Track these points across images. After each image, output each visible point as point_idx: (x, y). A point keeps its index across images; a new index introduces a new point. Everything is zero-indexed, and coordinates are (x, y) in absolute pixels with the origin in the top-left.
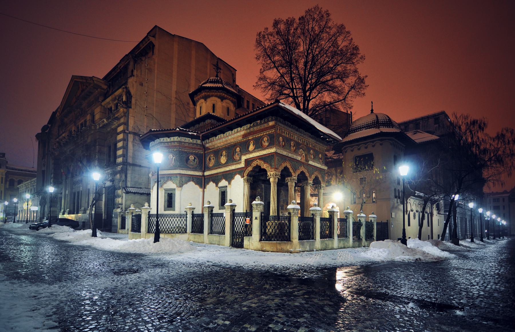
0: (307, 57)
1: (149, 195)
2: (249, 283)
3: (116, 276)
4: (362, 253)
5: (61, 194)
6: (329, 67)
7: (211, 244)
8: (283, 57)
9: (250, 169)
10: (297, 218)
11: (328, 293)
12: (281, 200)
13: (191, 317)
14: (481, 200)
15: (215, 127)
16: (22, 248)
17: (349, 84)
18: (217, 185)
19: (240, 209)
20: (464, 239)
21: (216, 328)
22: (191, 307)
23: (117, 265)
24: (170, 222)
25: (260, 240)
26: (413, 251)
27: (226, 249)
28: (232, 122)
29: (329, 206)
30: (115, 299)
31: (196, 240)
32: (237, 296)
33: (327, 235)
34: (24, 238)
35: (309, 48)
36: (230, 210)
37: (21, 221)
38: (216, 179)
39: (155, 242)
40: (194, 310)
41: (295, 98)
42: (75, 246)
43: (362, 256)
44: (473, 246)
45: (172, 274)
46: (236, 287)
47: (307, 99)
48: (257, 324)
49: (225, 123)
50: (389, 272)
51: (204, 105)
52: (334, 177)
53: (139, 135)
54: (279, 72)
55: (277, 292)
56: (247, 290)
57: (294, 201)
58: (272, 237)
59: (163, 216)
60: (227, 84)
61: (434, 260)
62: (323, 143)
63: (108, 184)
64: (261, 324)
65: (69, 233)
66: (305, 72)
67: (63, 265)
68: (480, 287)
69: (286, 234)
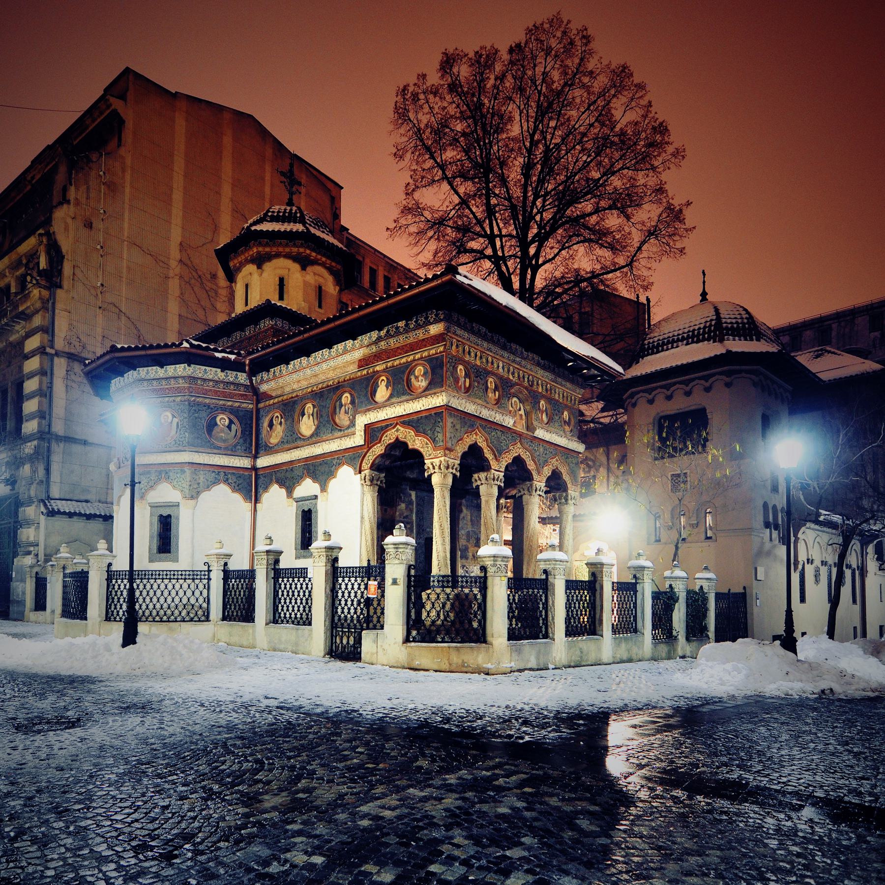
2: (377, 754)
10: (506, 580)
11: (587, 780)
12: (462, 533)
13: (222, 844)
15: (284, 340)
18: (290, 493)
19: (354, 555)
21: (286, 873)
24: (166, 593)
25: (407, 640)
28: (332, 325)
31: (235, 639)
32: (344, 789)
36: (324, 559)
39: (124, 645)
40: (230, 827)
45: (171, 730)
48: (397, 863)
49: (311, 329)
52: (603, 471)
55: (452, 779)
56: (371, 772)
57: (496, 536)
59: (146, 575)
62: (572, 382)
64: (408, 863)
69: (475, 625)
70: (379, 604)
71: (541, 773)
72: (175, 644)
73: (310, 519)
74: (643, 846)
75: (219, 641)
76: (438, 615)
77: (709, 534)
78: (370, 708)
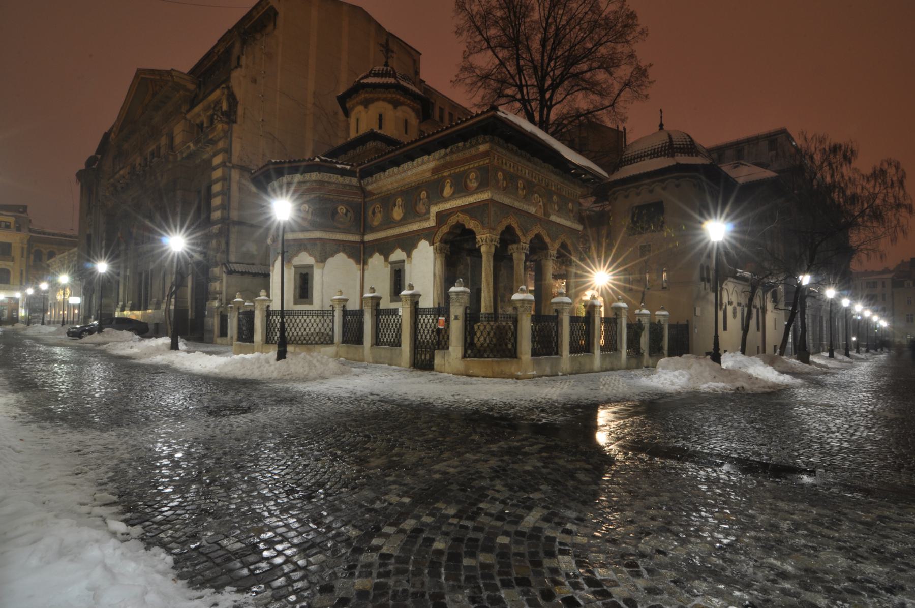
0: (545, 29)
1: (267, 276)
3: (212, 419)
5: (119, 274)
7: (377, 363)
8: (504, 30)
9: (445, 229)
10: (529, 317)
12: (501, 285)
14: (846, 282)
15: (382, 155)
16: (56, 367)
17: (621, 78)
18: (386, 259)
19: (428, 301)
20: (818, 352)
22: (343, 473)
23: (213, 399)
24: (305, 325)
30: (210, 458)
33: (582, 347)
34: (59, 352)
37: (54, 322)
41: (525, 102)
42: (143, 365)
43: (643, 384)
44: (832, 364)
45: (309, 415)
46: (421, 439)
47: (547, 105)
49: (400, 148)
50: (690, 412)
54: (497, 57)
57: (524, 287)
58: (485, 351)
59: (291, 313)
60: (404, 78)
63: (197, 257)
65: (132, 343)
66: (543, 57)
67: (124, 397)
68: (842, 434)
69: (510, 346)
71: (553, 443)
73: (400, 276)
74: (619, 490)
76: (485, 339)
77: (665, 285)
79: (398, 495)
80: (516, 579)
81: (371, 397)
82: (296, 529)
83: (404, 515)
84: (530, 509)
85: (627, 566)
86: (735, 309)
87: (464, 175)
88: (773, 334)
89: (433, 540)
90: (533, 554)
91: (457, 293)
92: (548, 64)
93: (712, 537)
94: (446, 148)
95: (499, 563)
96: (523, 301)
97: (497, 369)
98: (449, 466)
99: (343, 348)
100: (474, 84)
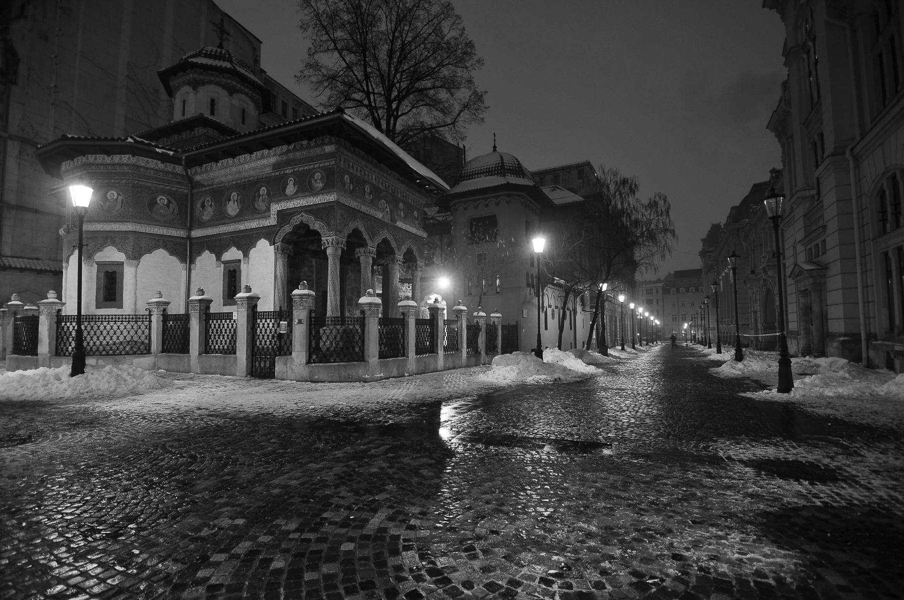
0: (392, 42)
1: (58, 274)
4: (481, 375)
6: (428, 67)
7: (206, 373)
8: (351, 35)
9: (288, 229)
12: (348, 288)
15: (214, 144)
19: (267, 305)
20: (613, 346)
22: (162, 501)
24: (112, 332)
25: (309, 362)
26: (550, 367)
27: (240, 382)
29: (430, 299)
31: (173, 367)
33: (427, 347)
35: (396, 29)
38: (217, 246)
39: (73, 374)
41: (372, 109)
43: (480, 380)
44: (623, 355)
47: (393, 115)
49: (236, 138)
51: (191, 97)
52: (438, 251)
53: (34, 145)
54: (344, 60)
57: (371, 290)
58: (331, 355)
59: (91, 318)
61: (578, 379)
66: (389, 68)
69: (357, 350)
70: (288, 338)
72: (120, 372)
73: (235, 277)
75: (159, 368)
76: (331, 343)
78: (281, 411)
79: (230, 518)
80: (361, 584)
81: (199, 412)
82: (96, 577)
83: (237, 539)
84: (375, 511)
85: (465, 550)
86: (553, 311)
87: (309, 174)
88: (582, 332)
89: (271, 560)
90: (377, 556)
91: (301, 296)
92: (395, 76)
93: (536, 511)
94: (289, 144)
95: (343, 571)
96: (370, 304)
97: (343, 373)
98: (290, 479)
99: (163, 360)
100: (320, 83)
